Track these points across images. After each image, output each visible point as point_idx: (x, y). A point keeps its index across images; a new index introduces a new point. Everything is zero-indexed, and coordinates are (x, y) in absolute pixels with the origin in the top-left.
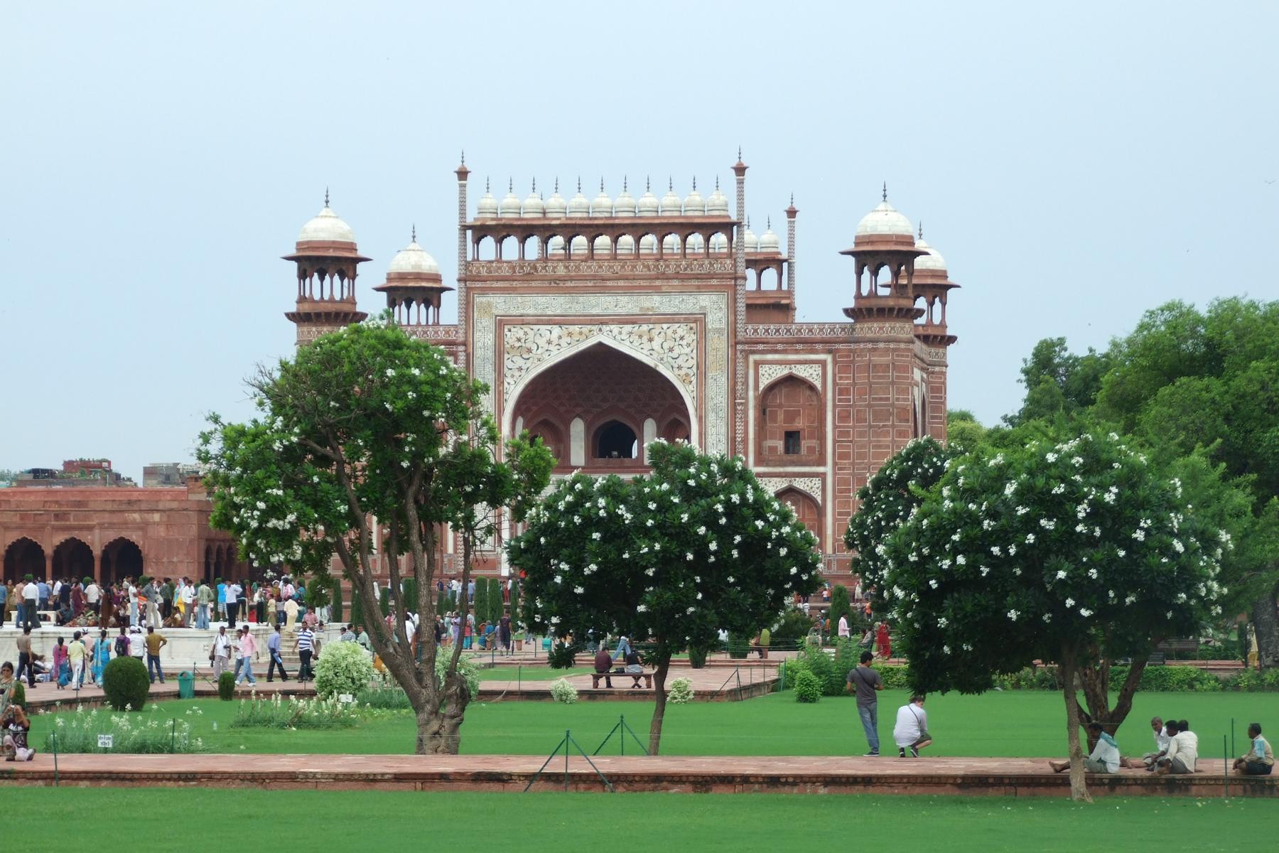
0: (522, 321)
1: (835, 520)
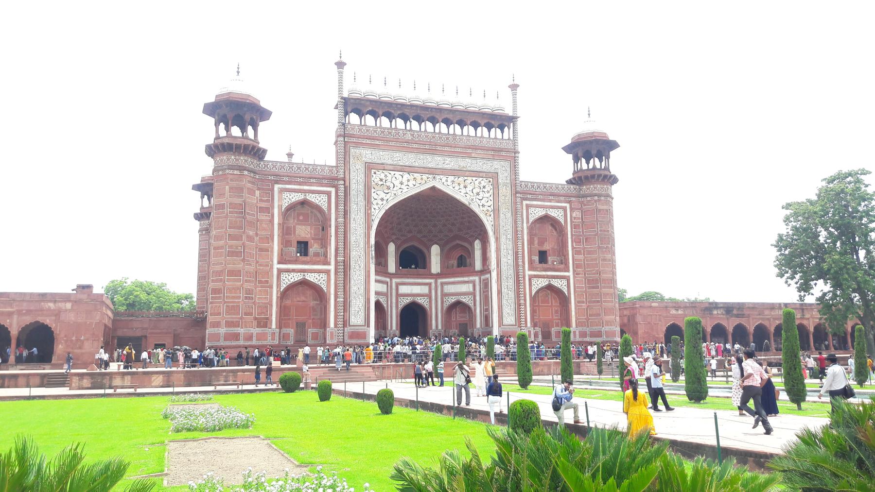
0: (383, 167)
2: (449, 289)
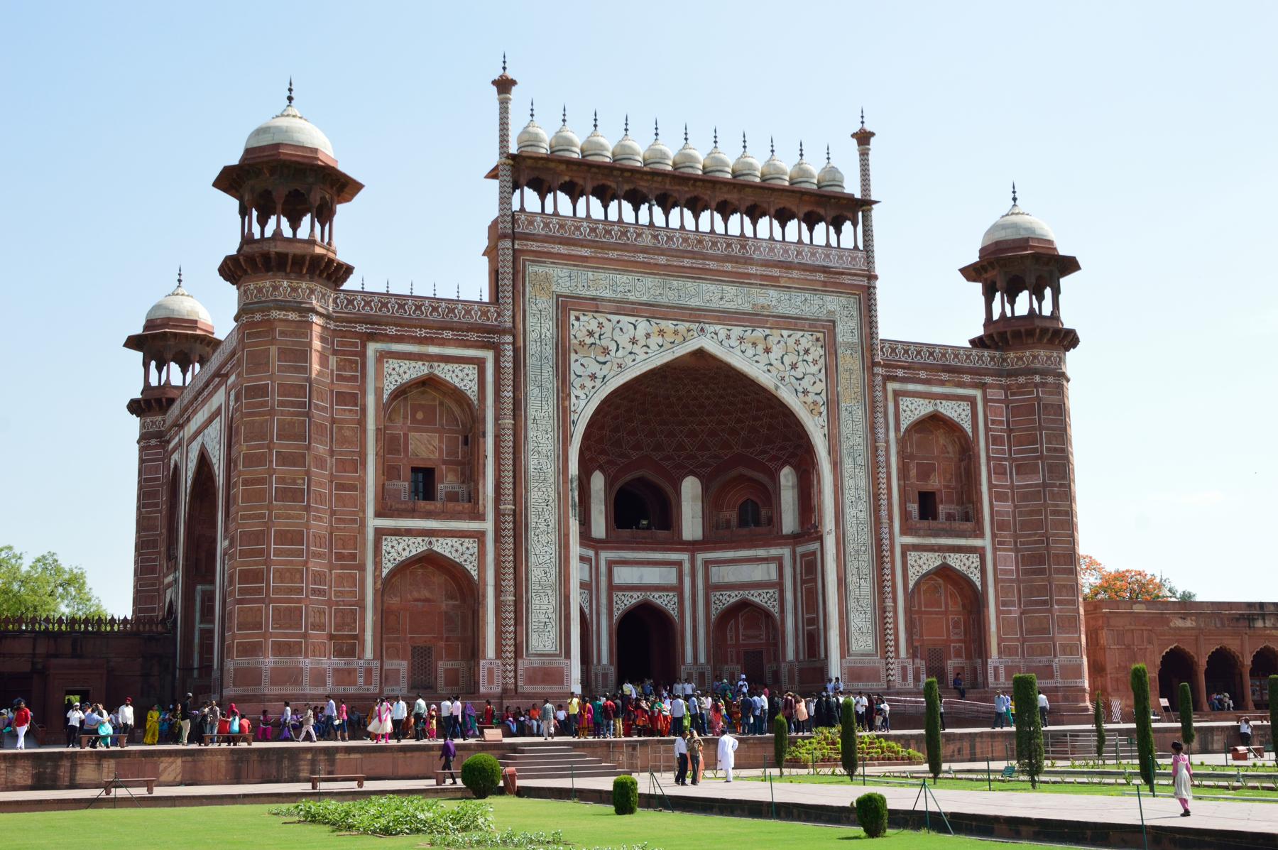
0: (593, 305)
1: (998, 612)
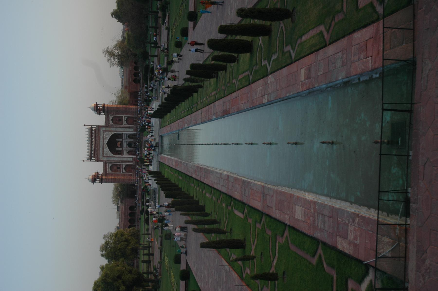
0: (103, 154)
2: (125, 137)
